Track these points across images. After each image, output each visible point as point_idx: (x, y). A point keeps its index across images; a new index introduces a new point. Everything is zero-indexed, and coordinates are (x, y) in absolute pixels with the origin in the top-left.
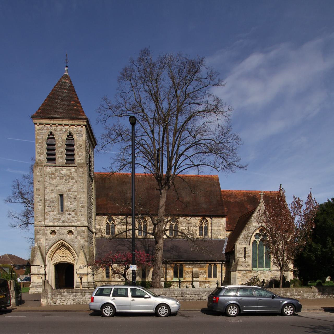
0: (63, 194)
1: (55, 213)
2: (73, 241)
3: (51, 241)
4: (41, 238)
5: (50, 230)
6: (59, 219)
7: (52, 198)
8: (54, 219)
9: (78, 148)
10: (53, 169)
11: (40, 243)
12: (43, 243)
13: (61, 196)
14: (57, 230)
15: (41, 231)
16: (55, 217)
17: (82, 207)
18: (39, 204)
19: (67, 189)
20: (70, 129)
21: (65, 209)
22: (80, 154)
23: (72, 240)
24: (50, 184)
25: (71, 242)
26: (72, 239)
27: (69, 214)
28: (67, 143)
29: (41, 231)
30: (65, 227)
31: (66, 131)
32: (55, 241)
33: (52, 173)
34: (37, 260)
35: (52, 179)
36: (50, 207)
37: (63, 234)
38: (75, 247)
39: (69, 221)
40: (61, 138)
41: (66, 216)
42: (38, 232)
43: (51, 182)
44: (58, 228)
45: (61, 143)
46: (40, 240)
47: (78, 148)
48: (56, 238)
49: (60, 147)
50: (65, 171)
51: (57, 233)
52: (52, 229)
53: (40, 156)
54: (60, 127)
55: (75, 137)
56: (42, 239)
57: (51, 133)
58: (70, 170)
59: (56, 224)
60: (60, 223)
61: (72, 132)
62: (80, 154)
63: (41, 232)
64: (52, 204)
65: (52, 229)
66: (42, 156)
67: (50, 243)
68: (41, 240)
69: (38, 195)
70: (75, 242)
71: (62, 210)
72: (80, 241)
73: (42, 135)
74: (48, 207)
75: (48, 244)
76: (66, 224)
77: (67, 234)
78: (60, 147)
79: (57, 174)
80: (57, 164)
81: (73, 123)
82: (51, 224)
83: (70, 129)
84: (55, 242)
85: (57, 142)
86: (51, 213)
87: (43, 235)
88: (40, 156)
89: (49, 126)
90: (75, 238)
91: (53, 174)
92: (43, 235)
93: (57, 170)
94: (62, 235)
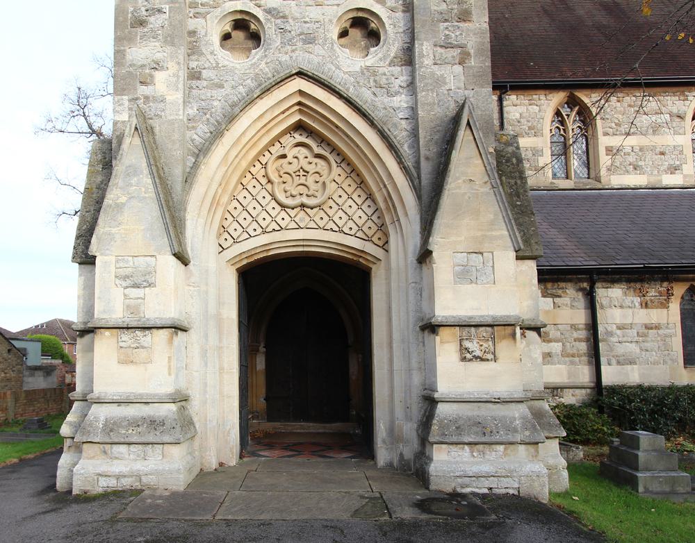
2: (383, 81)
3: (221, 86)
4: (157, 66)
5: (218, 12)
11: (147, 98)
12: (168, 98)
14: (269, 11)
15: (160, 11)
23: (374, 74)
25: (364, 96)
26: (370, 71)
29: (160, 11)
32: (252, 84)
37: (309, 39)
38: (395, 125)
46: (152, 76)
48: (263, 65)
51: (270, 30)
56: (162, 69)
63: (156, 21)
67: (219, 102)
68: (159, 76)
70: (397, 93)
72: (433, 74)
75: (203, 111)
77: (335, 36)
84: (258, 92)
87: (173, 44)
90: (392, 64)
92: (170, 40)
94: (306, 42)
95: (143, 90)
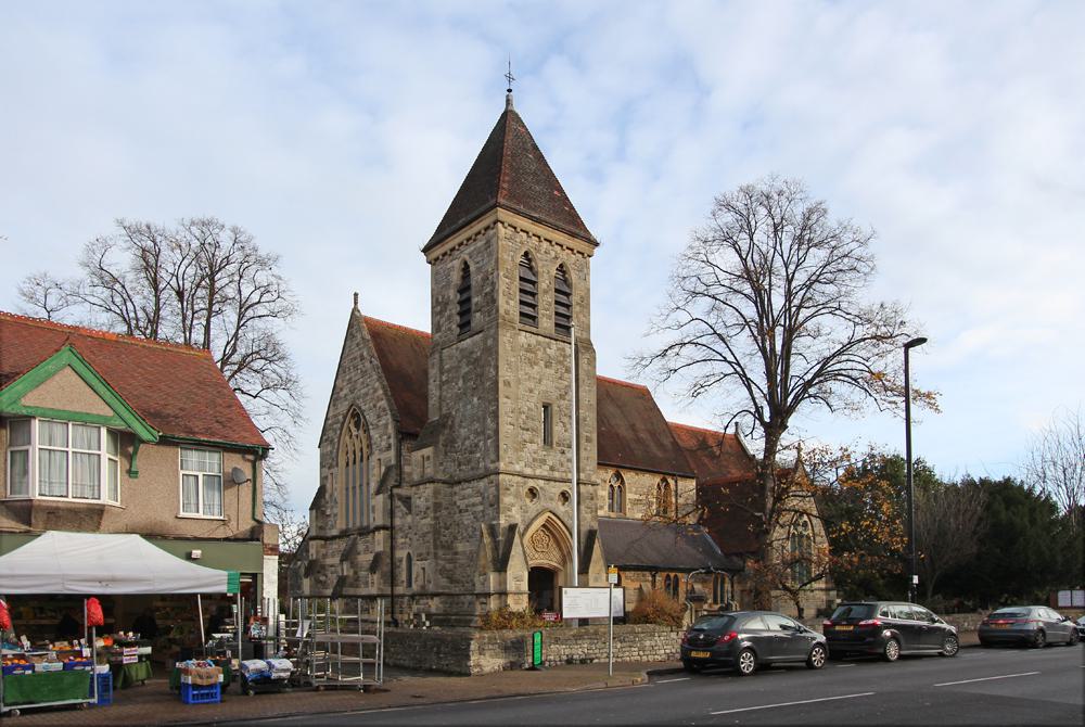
0: (550, 404)
1: (534, 446)
4: (513, 505)
6: (543, 462)
7: (529, 409)
8: (534, 460)
9: (578, 304)
10: (533, 339)
13: (546, 407)
16: (535, 456)
17: (588, 440)
18: (509, 419)
19: (557, 393)
20: (565, 256)
21: (555, 440)
22: (581, 316)
24: (526, 374)
27: (563, 453)
28: (557, 287)
30: (555, 481)
31: (556, 258)
33: (529, 349)
34: (515, 559)
35: (532, 363)
36: (528, 430)
39: (563, 469)
40: (549, 272)
41: (553, 458)
42: (508, 489)
43: (528, 369)
44: (541, 482)
45: (547, 282)
47: (578, 304)
49: (546, 292)
50: (554, 348)
52: (531, 483)
53: (507, 303)
54: (545, 245)
55: (574, 276)
57: (526, 254)
58: (563, 350)
59: (538, 472)
60: (543, 471)
61: (568, 263)
62: (581, 316)
64: (530, 424)
65: (531, 483)
66: (512, 303)
69: (507, 397)
71: (548, 441)
73: (512, 253)
74: (523, 429)
76: (557, 475)
78: (546, 292)
79: (540, 354)
80: (540, 331)
81: (571, 246)
82: (528, 471)
83: (565, 256)
85: (540, 279)
86: (529, 445)
88: (507, 303)
89: (524, 235)
91: (532, 352)
93: (539, 343)
95: (509, 513)
